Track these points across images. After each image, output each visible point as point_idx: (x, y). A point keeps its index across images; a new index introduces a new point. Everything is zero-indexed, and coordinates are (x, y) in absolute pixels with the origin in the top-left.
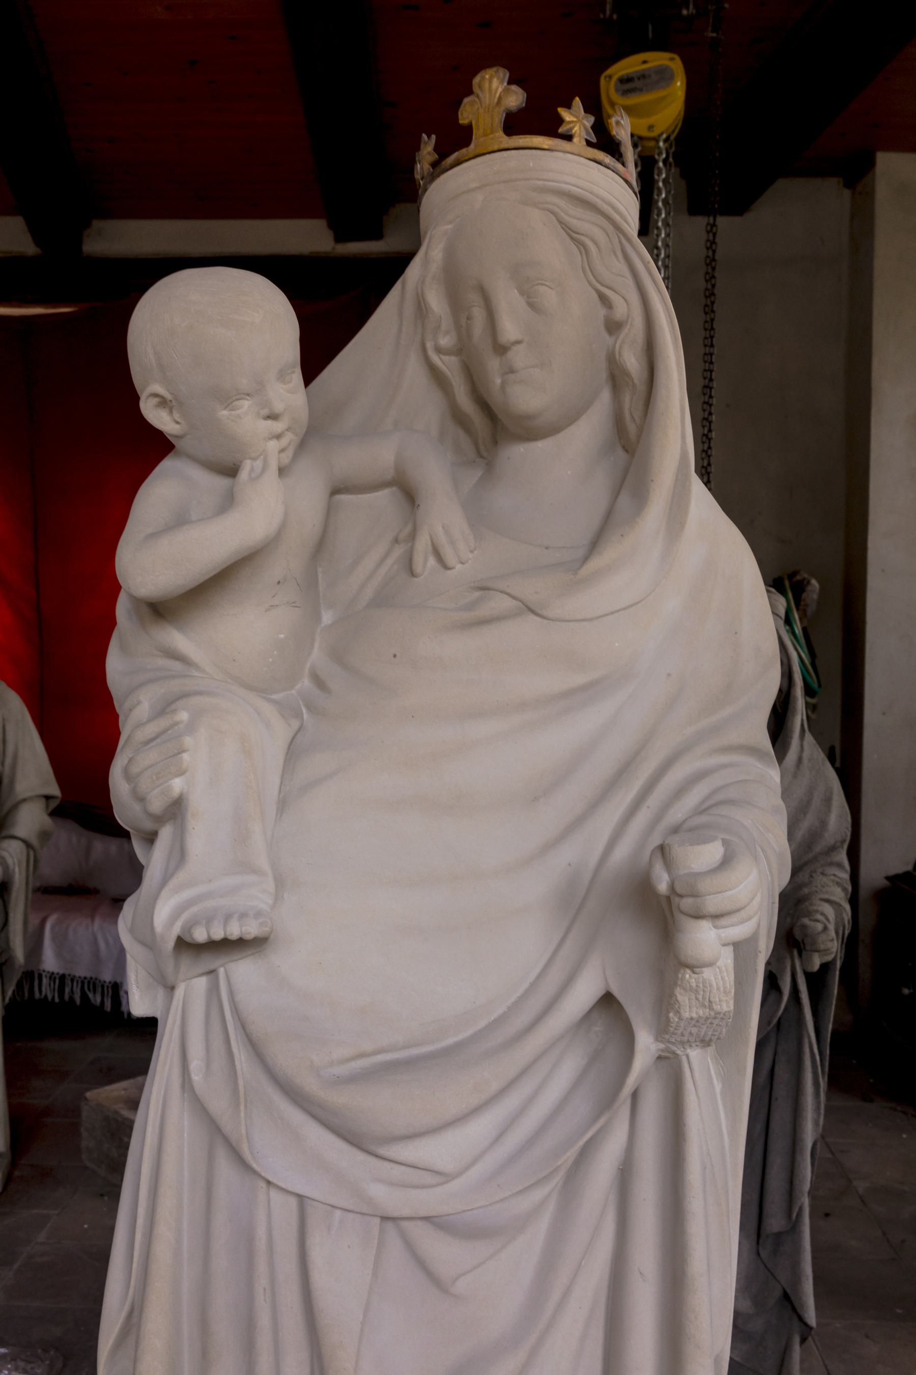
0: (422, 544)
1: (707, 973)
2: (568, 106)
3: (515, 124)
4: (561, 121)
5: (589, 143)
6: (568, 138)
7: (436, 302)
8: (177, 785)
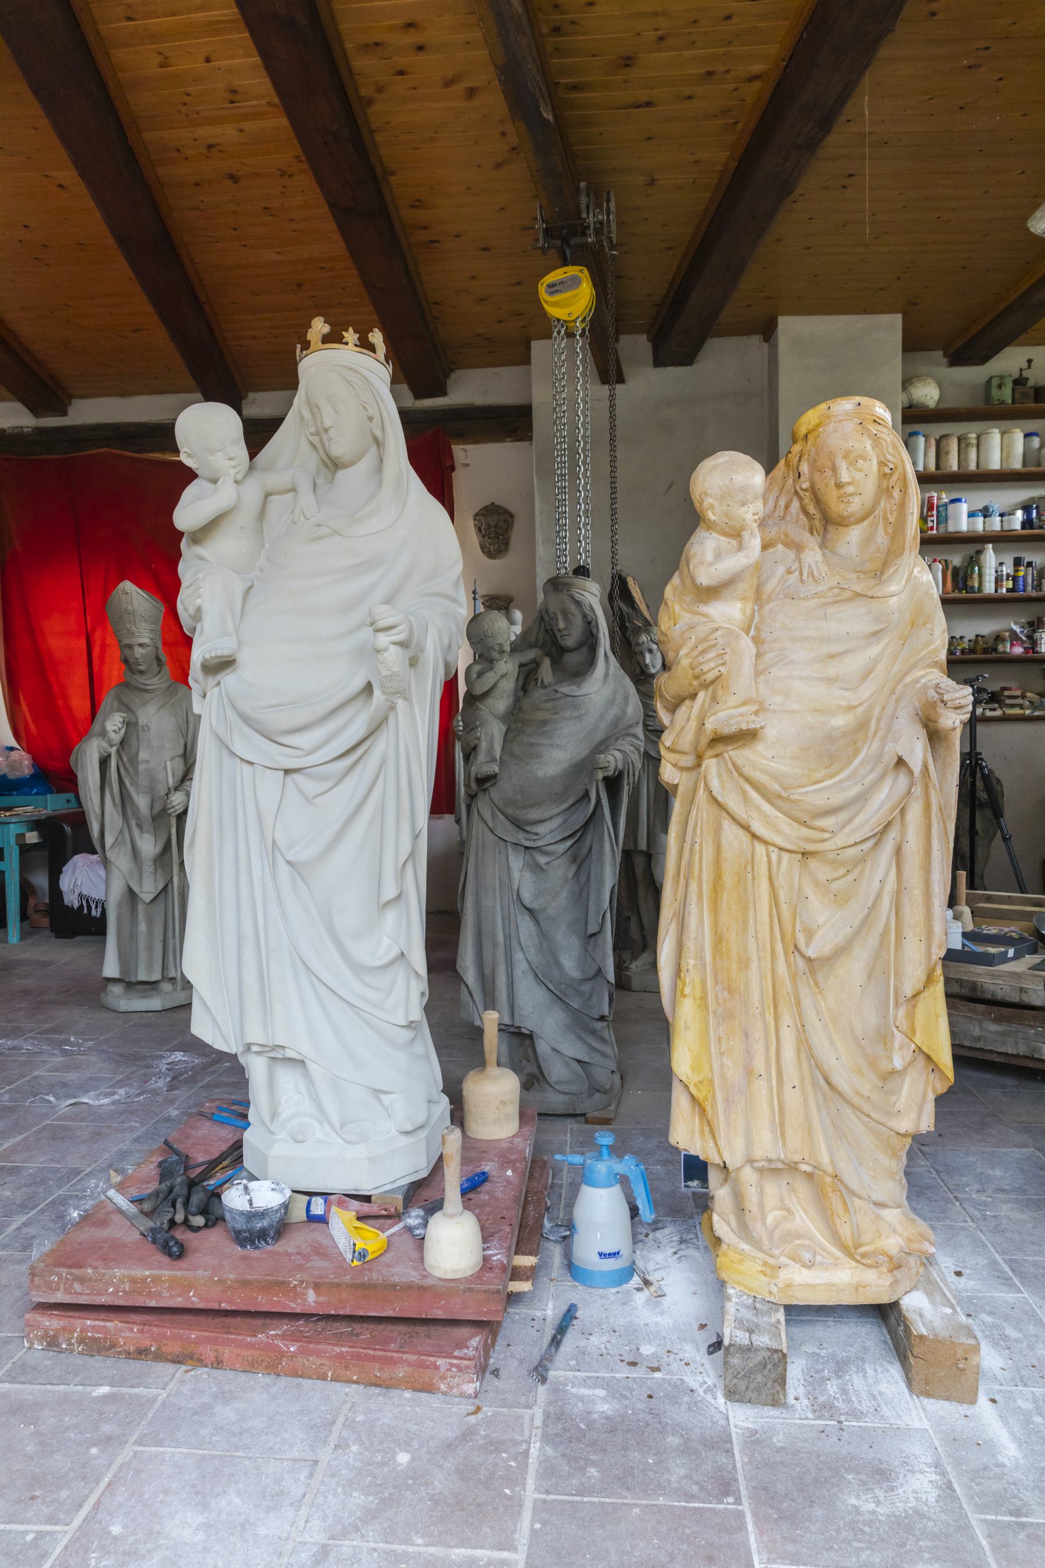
0: (297, 510)
1: (386, 654)
2: (347, 331)
3: (326, 339)
4: (343, 337)
5: (356, 345)
6: (347, 344)
7: (306, 414)
8: (198, 601)
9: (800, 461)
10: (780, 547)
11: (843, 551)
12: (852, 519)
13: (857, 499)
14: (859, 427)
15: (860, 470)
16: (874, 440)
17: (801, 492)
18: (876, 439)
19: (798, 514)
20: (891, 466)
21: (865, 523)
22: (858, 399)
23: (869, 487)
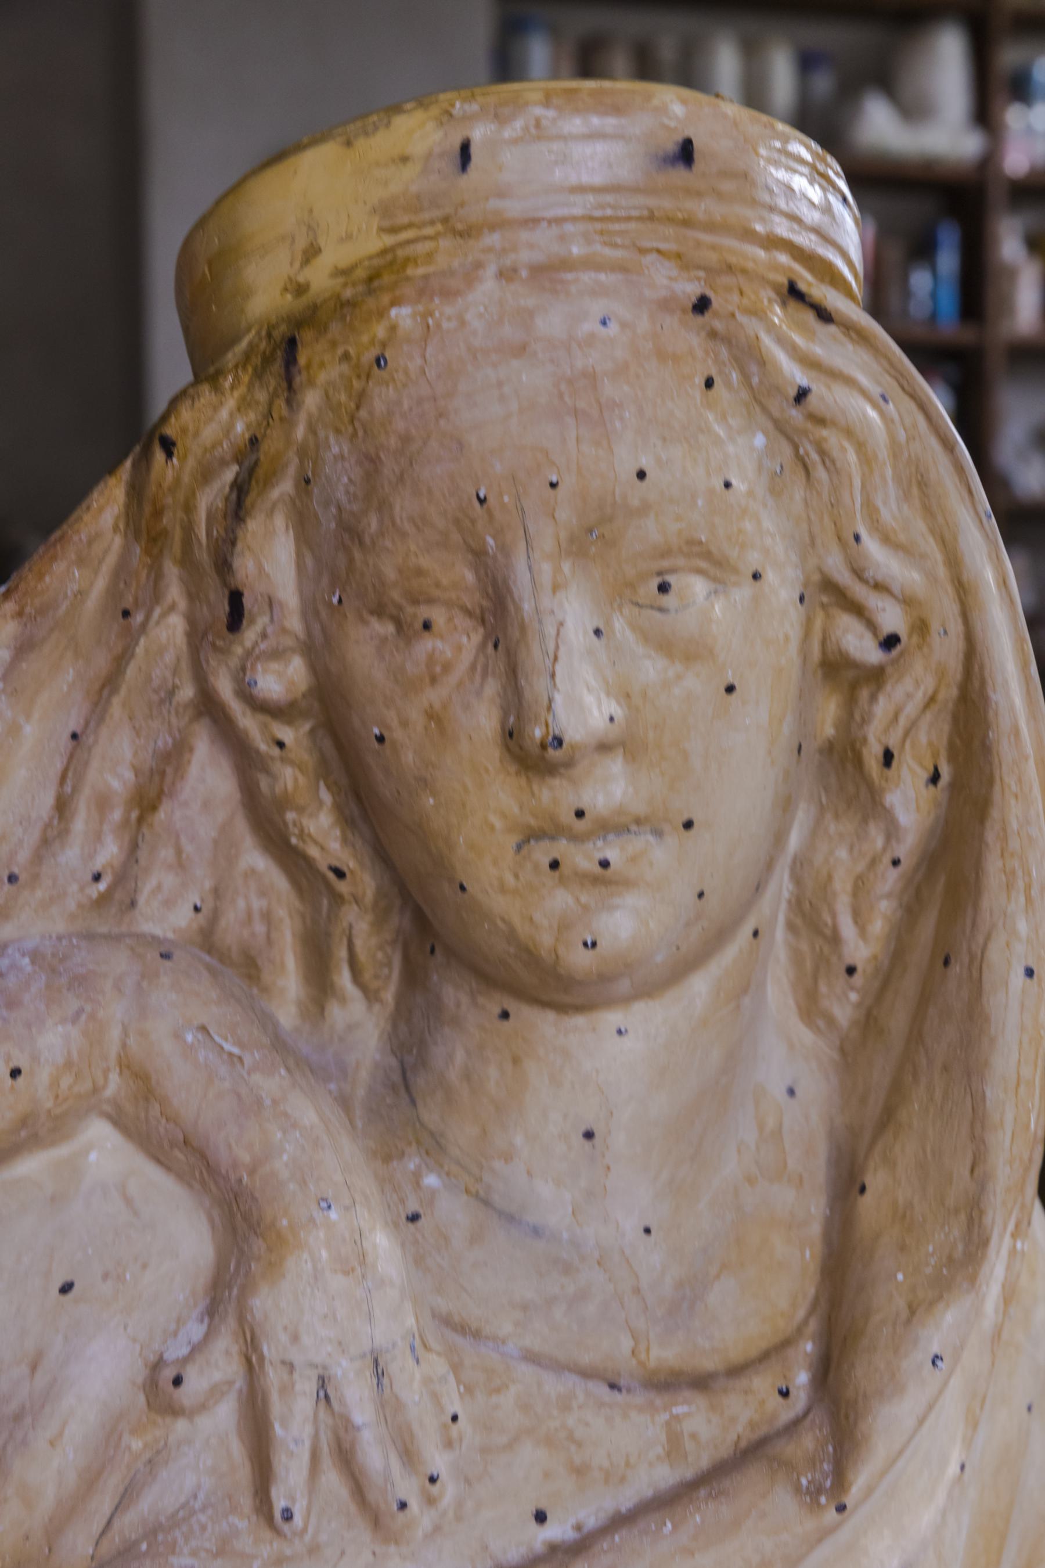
9: (239, 505)
10: (101, 1149)
11: (551, 1200)
12: (624, 986)
13: (660, 854)
14: (686, 336)
15: (685, 651)
16: (781, 427)
17: (247, 722)
18: (797, 421)
19: (224, 850)
20: (892, 618)
21: (700, 986)
22: (673, 107)
23: (744, 763)
